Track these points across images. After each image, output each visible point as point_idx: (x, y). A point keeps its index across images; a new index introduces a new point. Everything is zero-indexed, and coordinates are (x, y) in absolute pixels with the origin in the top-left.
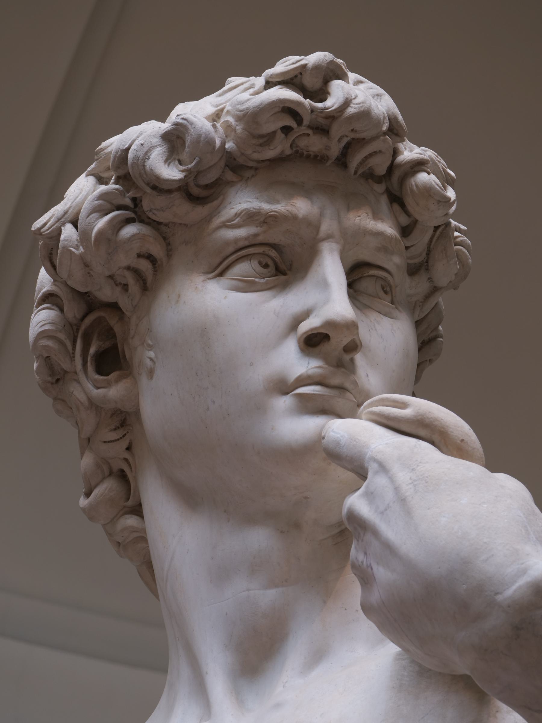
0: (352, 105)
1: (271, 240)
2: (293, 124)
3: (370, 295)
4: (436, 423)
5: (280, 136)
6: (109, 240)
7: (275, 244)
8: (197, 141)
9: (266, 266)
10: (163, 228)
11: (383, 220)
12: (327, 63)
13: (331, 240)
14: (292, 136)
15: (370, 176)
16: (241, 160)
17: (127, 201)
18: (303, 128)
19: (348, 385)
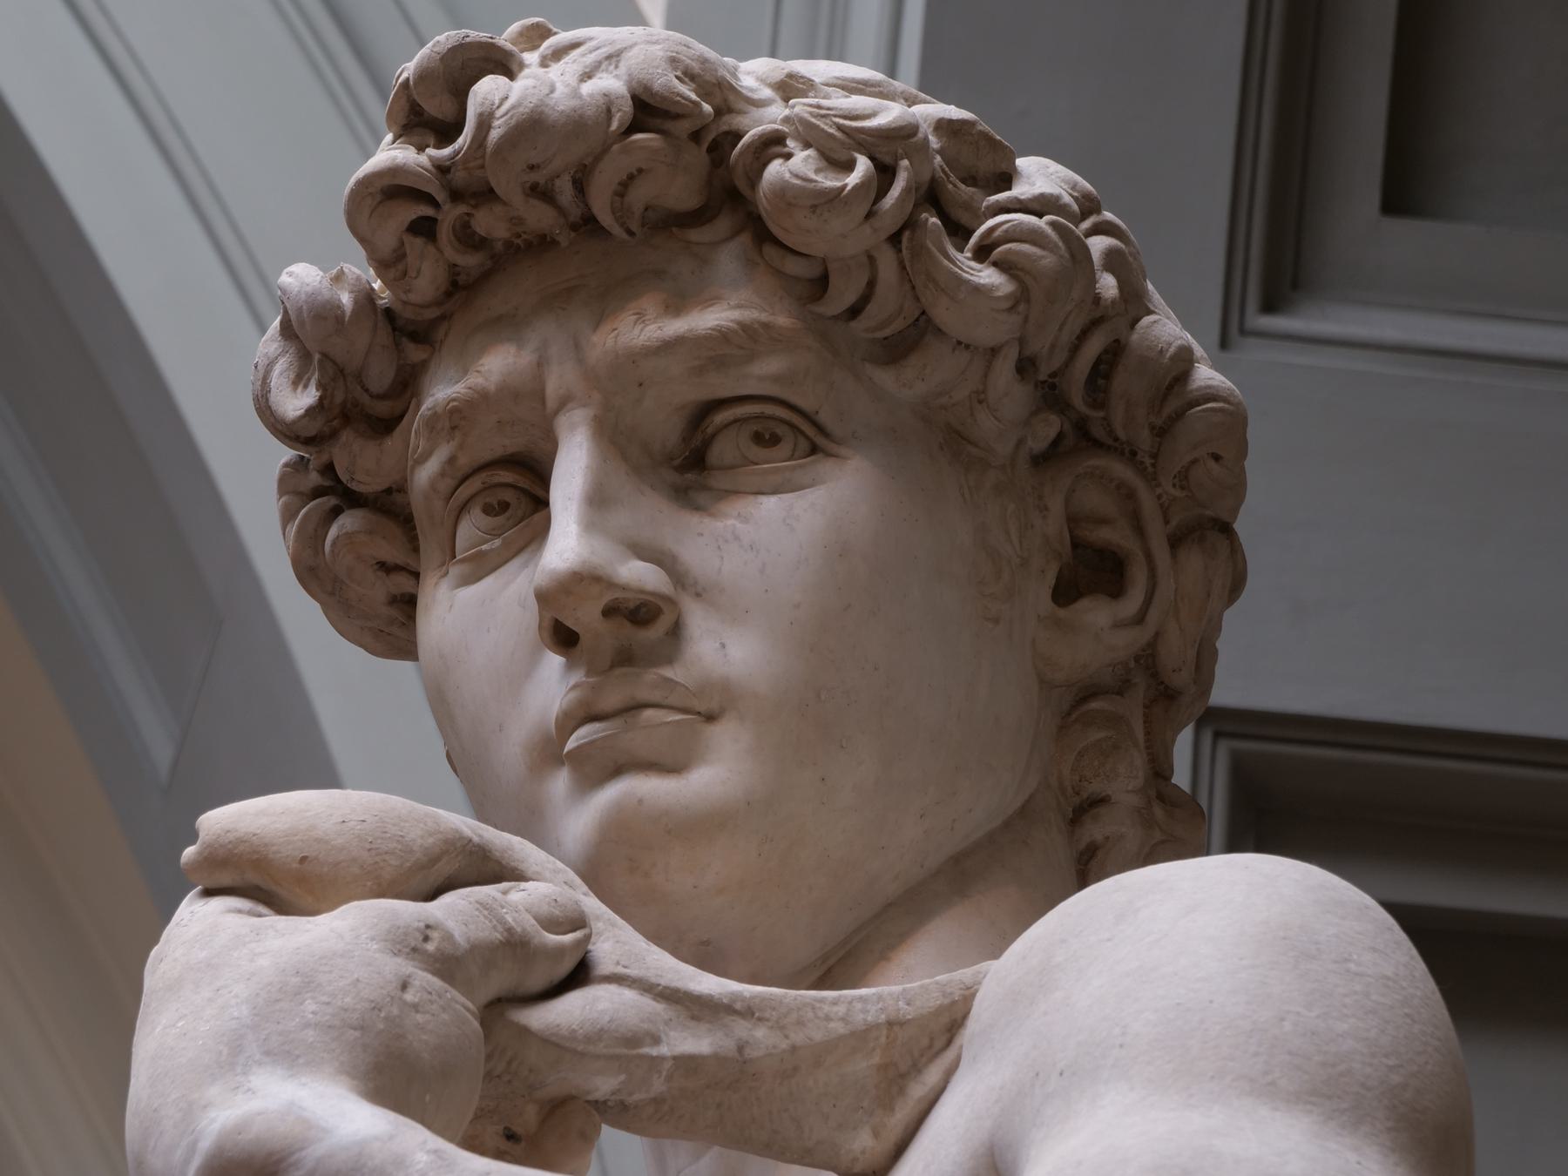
0: (496, 123)
1: (487, 455)
2: (428, 211)
3: (732, 467)
4: (241, 848)
5: (415, 244)
6: (312, 571)
7: (512, 455)
8: (302, 323)
9: (504, 506)
10: (398, 498)
11: (711, 301)
12: (442, 59)
13: (570, 406)
14: (444, 232)
15: (671, 223)
16: (408, 314)
17: (314, 479)
18: (446, 207)
19: (643, 694)
